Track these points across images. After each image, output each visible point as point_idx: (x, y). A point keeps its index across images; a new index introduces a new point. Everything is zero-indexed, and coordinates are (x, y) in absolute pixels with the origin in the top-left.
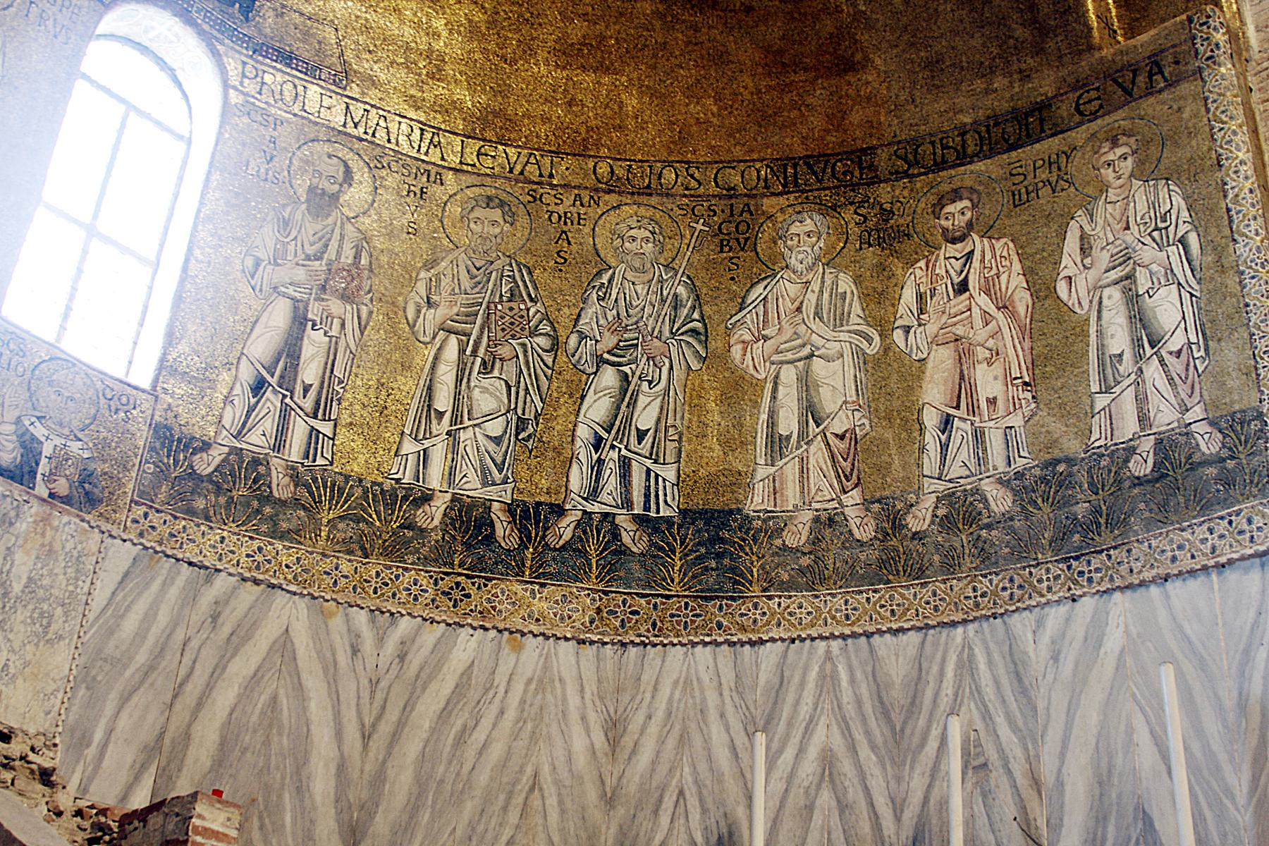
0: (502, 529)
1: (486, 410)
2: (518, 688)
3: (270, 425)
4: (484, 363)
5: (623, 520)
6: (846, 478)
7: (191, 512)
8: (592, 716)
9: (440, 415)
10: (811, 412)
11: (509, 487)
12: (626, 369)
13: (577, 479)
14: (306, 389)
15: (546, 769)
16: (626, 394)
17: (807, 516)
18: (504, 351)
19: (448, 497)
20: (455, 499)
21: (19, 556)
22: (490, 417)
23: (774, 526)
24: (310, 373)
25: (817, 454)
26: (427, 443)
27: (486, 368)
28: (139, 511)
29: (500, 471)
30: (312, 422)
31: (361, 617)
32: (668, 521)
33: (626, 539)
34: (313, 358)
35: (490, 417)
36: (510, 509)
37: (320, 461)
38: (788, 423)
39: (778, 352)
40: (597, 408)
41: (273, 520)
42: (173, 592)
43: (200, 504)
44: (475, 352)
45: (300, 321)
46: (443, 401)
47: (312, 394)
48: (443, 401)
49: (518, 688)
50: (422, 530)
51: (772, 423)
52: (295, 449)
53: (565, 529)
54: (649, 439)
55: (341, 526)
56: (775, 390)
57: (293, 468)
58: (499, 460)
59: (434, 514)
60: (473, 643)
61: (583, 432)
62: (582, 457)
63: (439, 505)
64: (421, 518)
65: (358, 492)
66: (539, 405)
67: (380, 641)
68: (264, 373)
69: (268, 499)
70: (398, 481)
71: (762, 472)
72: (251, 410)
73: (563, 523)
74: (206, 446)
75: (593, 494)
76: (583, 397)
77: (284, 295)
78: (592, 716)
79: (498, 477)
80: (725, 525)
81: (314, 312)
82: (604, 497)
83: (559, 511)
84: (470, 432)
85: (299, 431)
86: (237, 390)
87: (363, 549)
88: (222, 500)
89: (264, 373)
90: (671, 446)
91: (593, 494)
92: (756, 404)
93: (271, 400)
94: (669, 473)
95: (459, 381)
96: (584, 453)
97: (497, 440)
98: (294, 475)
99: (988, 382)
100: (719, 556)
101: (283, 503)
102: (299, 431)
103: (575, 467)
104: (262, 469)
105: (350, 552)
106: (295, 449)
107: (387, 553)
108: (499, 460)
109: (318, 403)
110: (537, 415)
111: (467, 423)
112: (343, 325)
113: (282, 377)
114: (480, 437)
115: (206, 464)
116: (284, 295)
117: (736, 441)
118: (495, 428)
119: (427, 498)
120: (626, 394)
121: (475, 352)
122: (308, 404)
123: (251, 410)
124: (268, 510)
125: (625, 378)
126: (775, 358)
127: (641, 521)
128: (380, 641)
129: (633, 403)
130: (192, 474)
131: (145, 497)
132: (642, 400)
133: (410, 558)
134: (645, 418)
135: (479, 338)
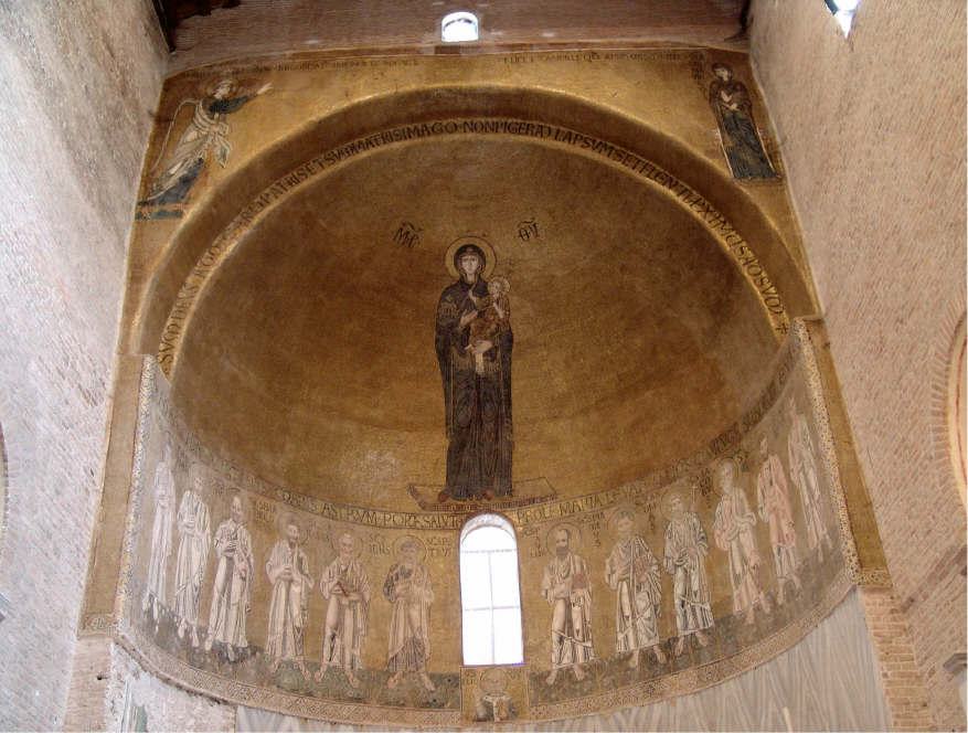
0: (660, 657)
3: (569, 654)
5: (698, 635)
6: (760, 587)
7: (551, 701)
10: (744, 561)
11: (658, 638)
13: (679, 623)
17: (751, 609)
18: (643, 579)
20: (640, 650)
22: (645, 610)
23: (744, 616)
24: (577, 625)
25: (749, 580)
28: (533, 710)
31: (619, 715)
32: (711, 628)
33: (700, 641)
35: (645, 610)
36: (660, 646)
38: (739, 569)
41: (581, 690)
43: (553, 696)
45: (568, 606)
46: (627, 612)
47: (580, 633)
48: (627, 612)
51: (734, 569)
53: (680, 646)
59: (635, 662)
61: (677, 601)
64: (631, 664)
67: (628, 721)
69: (577, 682)
71: (735, 593)
74: (549, 673)
75: (686, 627)
80: (729, 623)
81: (573, 600)
82: (690, 627)
83: (676, 639)
91: (686, 627)
93: (567, 643)
94: (708, 607)
95: (631, 600)
96: (679, 610)
97: (649, 619)
98: (583, 668)
99: (786, 530)
100: (730, 638)
107: (623, 684)
109: (583, 636)
115: (551, 680)
117: (726, 584)
119: (631, 655)
122: (580, 638)
124: (578, 687)
127: (704, 631)
128: (628, 721)
130: (547, 686)
131: (534, 703)
133: (631, 682)
134: (695, 587)
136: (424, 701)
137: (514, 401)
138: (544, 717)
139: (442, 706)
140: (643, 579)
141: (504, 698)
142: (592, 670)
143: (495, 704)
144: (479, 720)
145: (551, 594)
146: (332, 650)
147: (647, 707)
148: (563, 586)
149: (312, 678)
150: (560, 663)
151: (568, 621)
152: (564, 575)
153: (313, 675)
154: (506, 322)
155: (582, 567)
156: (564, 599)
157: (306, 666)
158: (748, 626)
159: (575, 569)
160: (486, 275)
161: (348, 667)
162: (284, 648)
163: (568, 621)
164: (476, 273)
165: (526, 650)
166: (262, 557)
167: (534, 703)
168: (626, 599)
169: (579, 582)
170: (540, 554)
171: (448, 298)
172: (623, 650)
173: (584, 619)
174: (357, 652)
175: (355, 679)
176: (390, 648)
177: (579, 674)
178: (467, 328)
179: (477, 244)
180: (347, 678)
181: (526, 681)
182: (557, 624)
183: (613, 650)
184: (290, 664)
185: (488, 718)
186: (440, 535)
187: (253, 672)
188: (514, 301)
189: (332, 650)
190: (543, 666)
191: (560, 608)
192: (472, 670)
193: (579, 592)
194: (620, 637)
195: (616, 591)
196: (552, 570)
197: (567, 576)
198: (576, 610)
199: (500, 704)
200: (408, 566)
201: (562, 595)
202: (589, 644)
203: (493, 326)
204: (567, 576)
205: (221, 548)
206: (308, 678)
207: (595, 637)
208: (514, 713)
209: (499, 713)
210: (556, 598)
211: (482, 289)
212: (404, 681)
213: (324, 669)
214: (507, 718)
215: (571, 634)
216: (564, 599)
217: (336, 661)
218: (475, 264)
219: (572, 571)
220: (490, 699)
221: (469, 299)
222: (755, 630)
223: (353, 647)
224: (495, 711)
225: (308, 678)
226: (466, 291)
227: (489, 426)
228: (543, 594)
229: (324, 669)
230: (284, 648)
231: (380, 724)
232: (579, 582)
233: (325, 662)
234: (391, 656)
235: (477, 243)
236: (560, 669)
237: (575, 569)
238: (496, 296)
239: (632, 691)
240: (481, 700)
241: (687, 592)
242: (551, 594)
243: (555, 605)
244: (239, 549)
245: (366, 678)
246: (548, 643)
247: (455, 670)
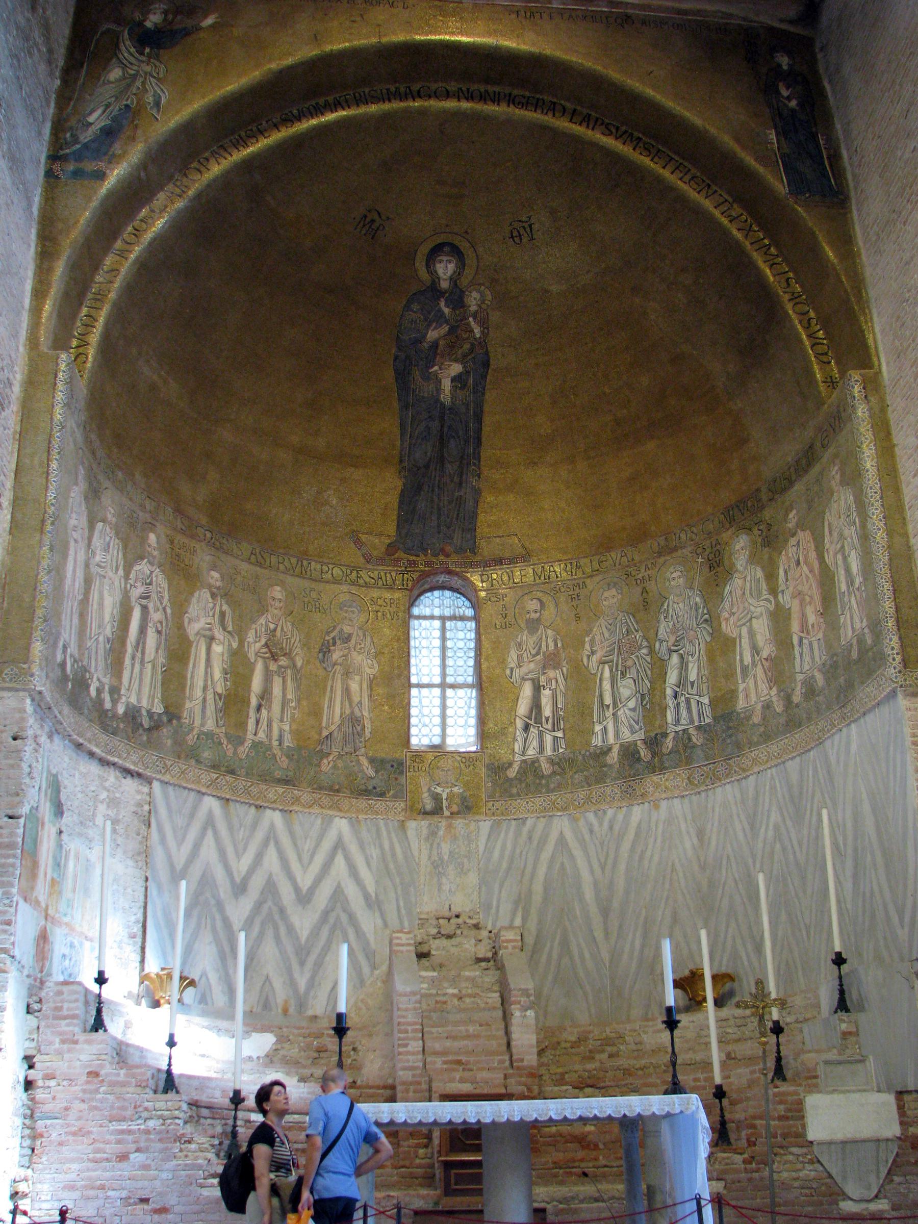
1: (626, 696)
2: (661, 827)
4: (622, 672)
7: (511, 796)
8: (691, 830)
9: (608, 706)
12: (681, 652)
15: (677, 861)
16: (683, 666)
19: (618, 746)
21: (443, 845)
24: (547, 711)
26: (605, 723)
27: (623, 674)
29: (638, 724)
30: (553, 734)
31: (591, 816)
34: (547, 704)
37: (561, 750)
39: (739, 620)
40: (672, 677)
41: (547, 785)
42: (511, 834)
44: (617, 670)
45: (537, 689)
48: (608, 700)
49: (661, 827)
50: (610, 765)
52: (549, 748)
54: (696, 685)
55: (576, 776)
56: (740, 641)
57: (550, 759)
58: (636, 719)
60: (639, 812)
62: (671, 705)
63: (615, 750)
65: (580, 758)
66: (649, 684)
68: (527, 720)
70: (596, 746)
73: (668, 741)
76: (666, 673)
77: (528, 679)
78: (691, 830)
79: (637, 727)
83: (665, 735)
84: (622, 711)
86: (518, 733)
87: (588, 783)
88: (523, 785)
89: (527, 720)
90: (705, 685)
92: (734, 651)
95: (612, 687)
101: (549, 776)
103: (668, 711)
104: (536, 765)
105: (583, 787)
106: (549, 748)
108: (636, 719)
109: (554, 725)
110: (649, 690)
111: (620, 706)
112: (557, 681)
113: (535, 718)
114: (627, 711)
116: (528, 679)
118: (632, 704)
120: (683, 666)
121: (617, 670)
125: (682, 657)
126: (739, 623)
129: (687, 669)
131: (491, 797)
132: (690, 665)
133: (608, 781)
135: (617, 661)
136: (364, 788)
137: (483, 440)
138: (503, 814)
139: (382, 795)
140: (629, 663)
141: (456, 790)
142: (561, 764)
143: (444, 796)
144: (426, 813)
145: (517, 673)
147: (624, 809)
148: (532, 666)
151: (536, 705)
152: (533, 652)
154: (483, 343)
155: (556, 645)
156: (533, 680)
159: (547, 646)
160: (464, 282)
163: (536, 705)
164: (451, 279)
165: (483, 735)
166: (180, 607)
167: (491, 797)
168: (607, 685)
169: (551, 661)
170: (505, 627)
171: (415, 307)
173: (555, 703)
177: (546, 768)
178: (435, 345)
179: (456, 242)
181: (483, 771)
182: (523, 708)
183: (588, 743)
185: (437, 811)
186: (388, 595)
188: (495, 317)
190: (503, 754)
191: (527, 691)
192: (418, 756)
193: (551, 673)
194: (598, 728)
195: (595, 674)
196: (519, 645)
197: (538, 654)
198: (546, 694)
199: (451, 797)
200: (347, 629)
201: (530, 676)
203: (467, 346)
204: (538, 654)
205: (136, 593)
207: (568, 726)
208: (467, 807)
209: (448, 807)
210: (523, 679)
211: (457, 298)
212: (340, 764)
214: (458, 813)
215: (538, 721)
216: (533, 680)
218: (451, 267)
219: (544, 648)
220: (439, 790)
221: (440, 310)
224: (445, 803)
226: (439, 299)
227: (450, 468)
228: (508, 672)
231: (312, 811)
232: (551, 661)
235: (457, 241)
236: (524, 761)
237: (547, 646)
238: (473, 308)
239: (608, 791)
240: (429, 789)
241: (682, 682)
242: (517, 673)
243: (520, 688)
244: (154, 596)
247: (400, 754)
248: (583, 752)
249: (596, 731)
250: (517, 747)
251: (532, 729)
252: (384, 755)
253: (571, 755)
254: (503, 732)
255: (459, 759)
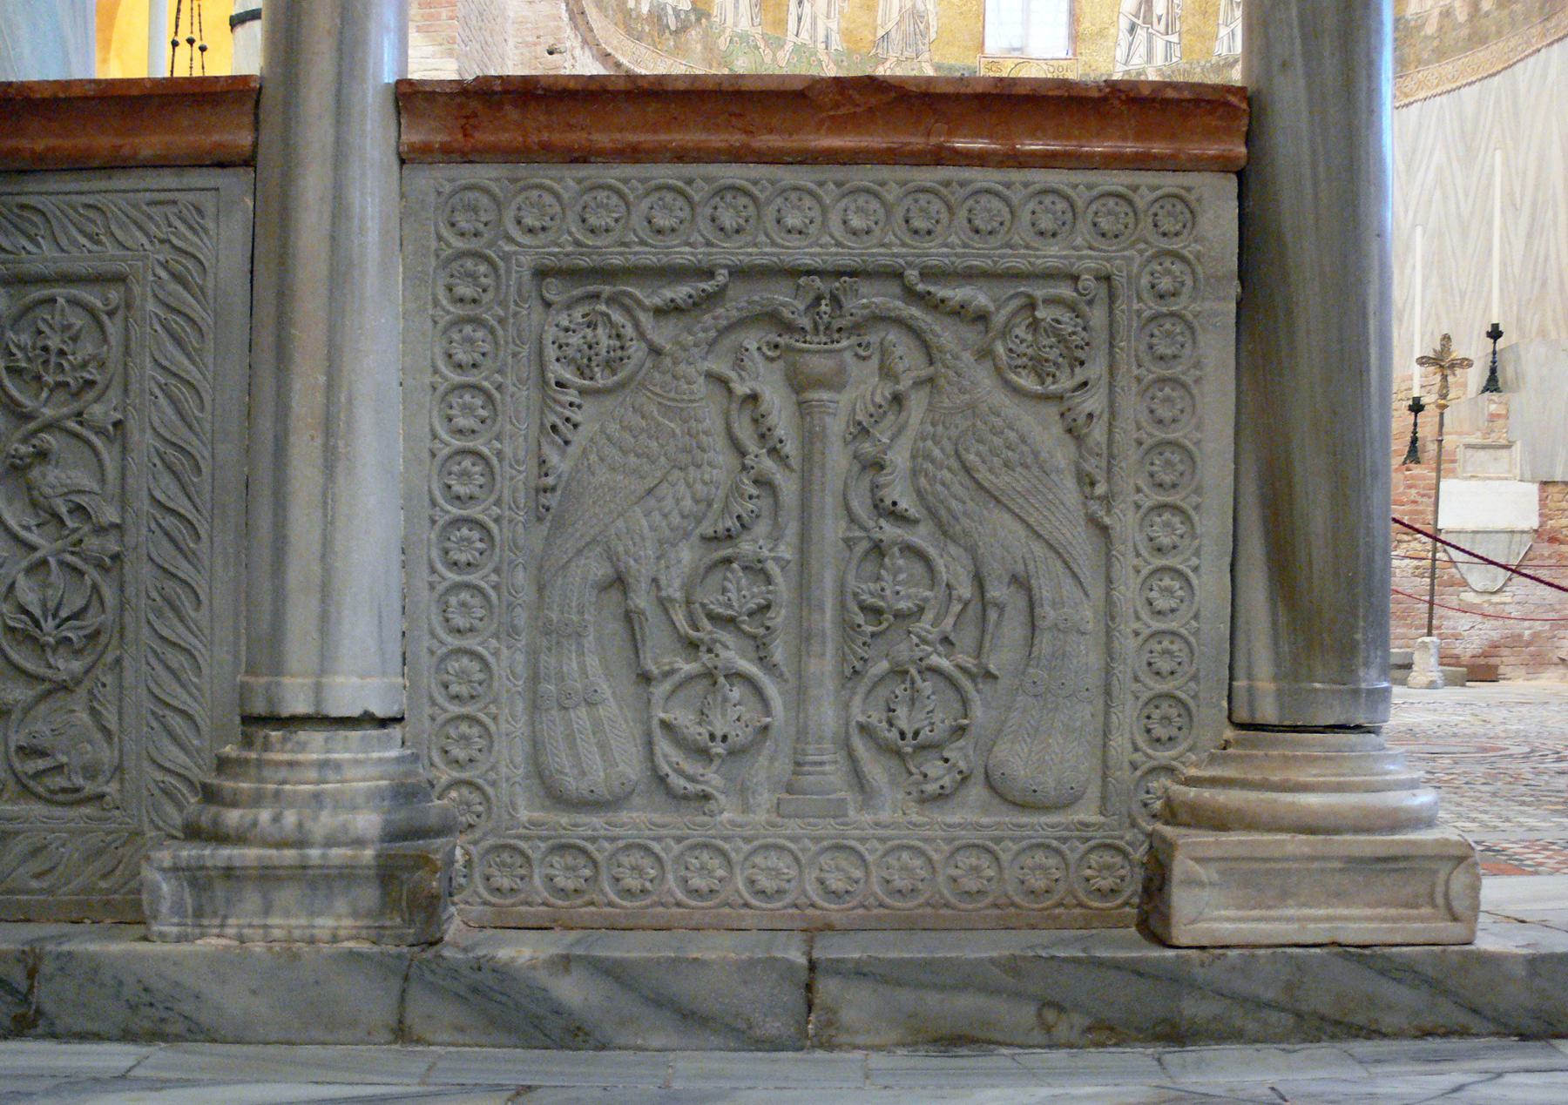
3: (1142, 50)
14: (1159, 20)
17: (1436, 12)
26: (1233, 26)
30: (1167, 38)
37: (1174, 60)
72: (1131, 44)
85: (1159, 45)
93: (1141, 34)
102: (1159, 45)
113: (1145, 17)
122: (1162, 28)
123: (1131, 44)
146: (800, 19)
149: (774, 59)
150: (1126, 63)
153: (774, 55)
157: (767, 45)
158: (1426, 37)
161: (821, 46)
162: (736, 14)
165: (1075, 37)
172: (1225, 52)
174: (834, 26)
175: (832, 65)
176: (879, 22)
180: (820, 61)
183: (1209, 52)
184: (744, 38)
187: (699, 47)
189: (800, 19)
194: (1223, 32)
202: (1174, 38)
206: (768, 60)
207: (1185, 28)
213: (789, 47)
217: (805, 36)
222: (1436, 43)
223: (828, 17)
225: (768, 60)
229: (789, 47)
230: (736, 14)
233: (791, 37)
234: (881, 33)
245: (845, 64)
246: (1112, 31)
248: (1202, 63)
249: (1220, 35)
250: (1120, 54)
251: (1139, 31)
252: (952, 62)
253: (1187, 66)
254: (1101, 33)
255: (1045, 67)
